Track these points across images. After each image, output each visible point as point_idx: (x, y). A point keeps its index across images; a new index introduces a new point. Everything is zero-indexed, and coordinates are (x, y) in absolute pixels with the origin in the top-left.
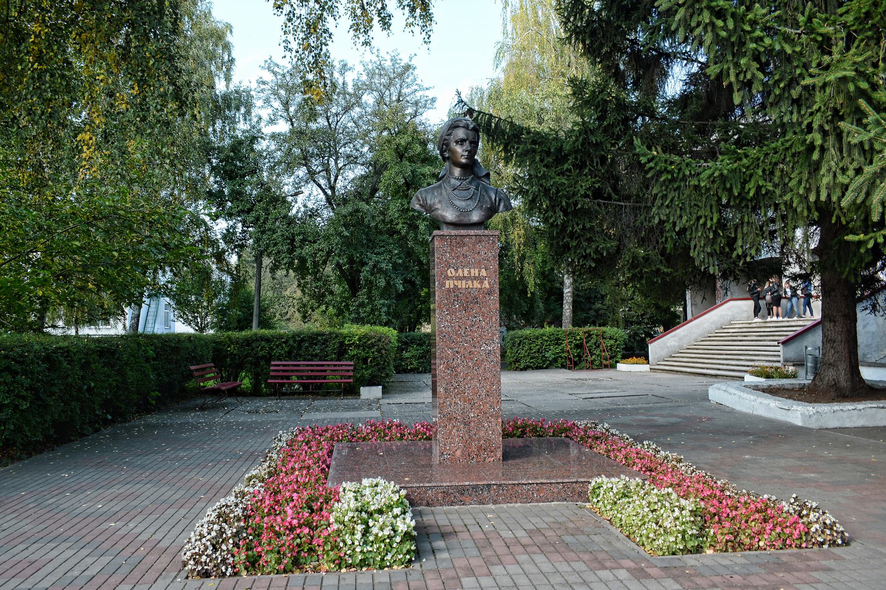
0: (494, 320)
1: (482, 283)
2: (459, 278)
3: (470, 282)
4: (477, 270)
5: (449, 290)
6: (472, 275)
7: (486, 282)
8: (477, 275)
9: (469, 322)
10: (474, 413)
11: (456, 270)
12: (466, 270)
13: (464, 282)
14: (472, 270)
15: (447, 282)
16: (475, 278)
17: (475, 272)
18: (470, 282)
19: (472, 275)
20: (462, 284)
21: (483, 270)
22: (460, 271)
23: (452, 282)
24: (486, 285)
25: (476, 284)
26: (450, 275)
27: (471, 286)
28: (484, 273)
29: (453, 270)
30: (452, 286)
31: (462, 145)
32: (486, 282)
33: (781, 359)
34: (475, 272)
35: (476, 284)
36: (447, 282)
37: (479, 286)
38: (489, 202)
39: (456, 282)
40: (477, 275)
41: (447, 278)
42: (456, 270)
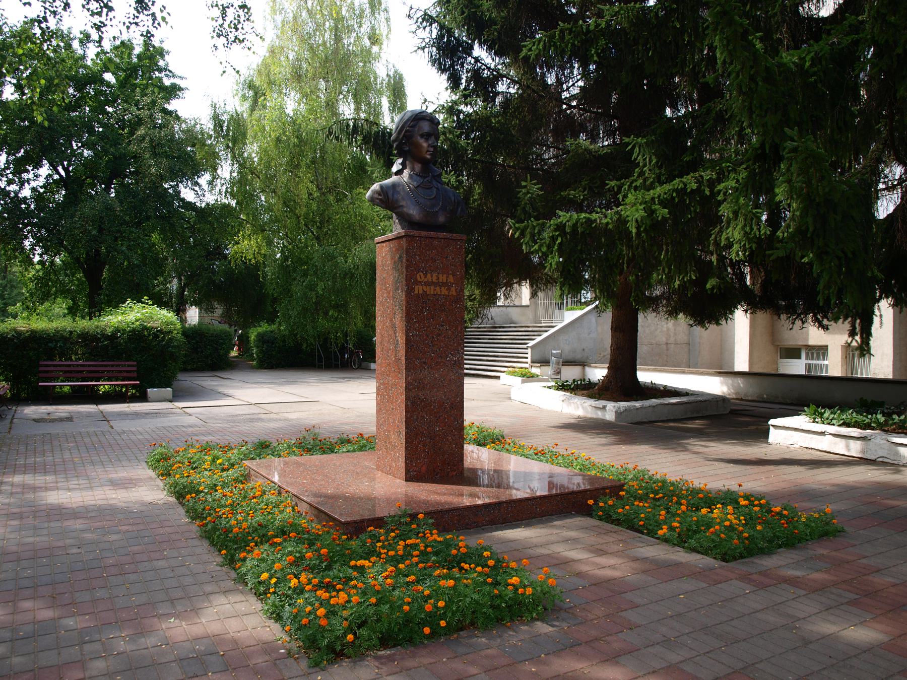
1: (449, 289)
2: (428, 284)
3: (438, 288)
5: (418, 295)
7: (453, 289)
10: (439, 426)
11: (425, 275)
12: (434, 275)
13: (432, 288)
15: (416, 287)
16: (444, 284)
17: (443, 278)
18: (438, 288)
20: (430, 290)
21: (451, 276)
22: (429, 275)
23: (421, 288)
25: (444, 291)
26: (419, 279)
28: (451, 279)
30: (421, 292)
31: (427, 140)
33: (529, 360)
34: (443, 278)
35: (444, 291)
36: (416, 287)
41: (417, 282)
42: (425, 275)
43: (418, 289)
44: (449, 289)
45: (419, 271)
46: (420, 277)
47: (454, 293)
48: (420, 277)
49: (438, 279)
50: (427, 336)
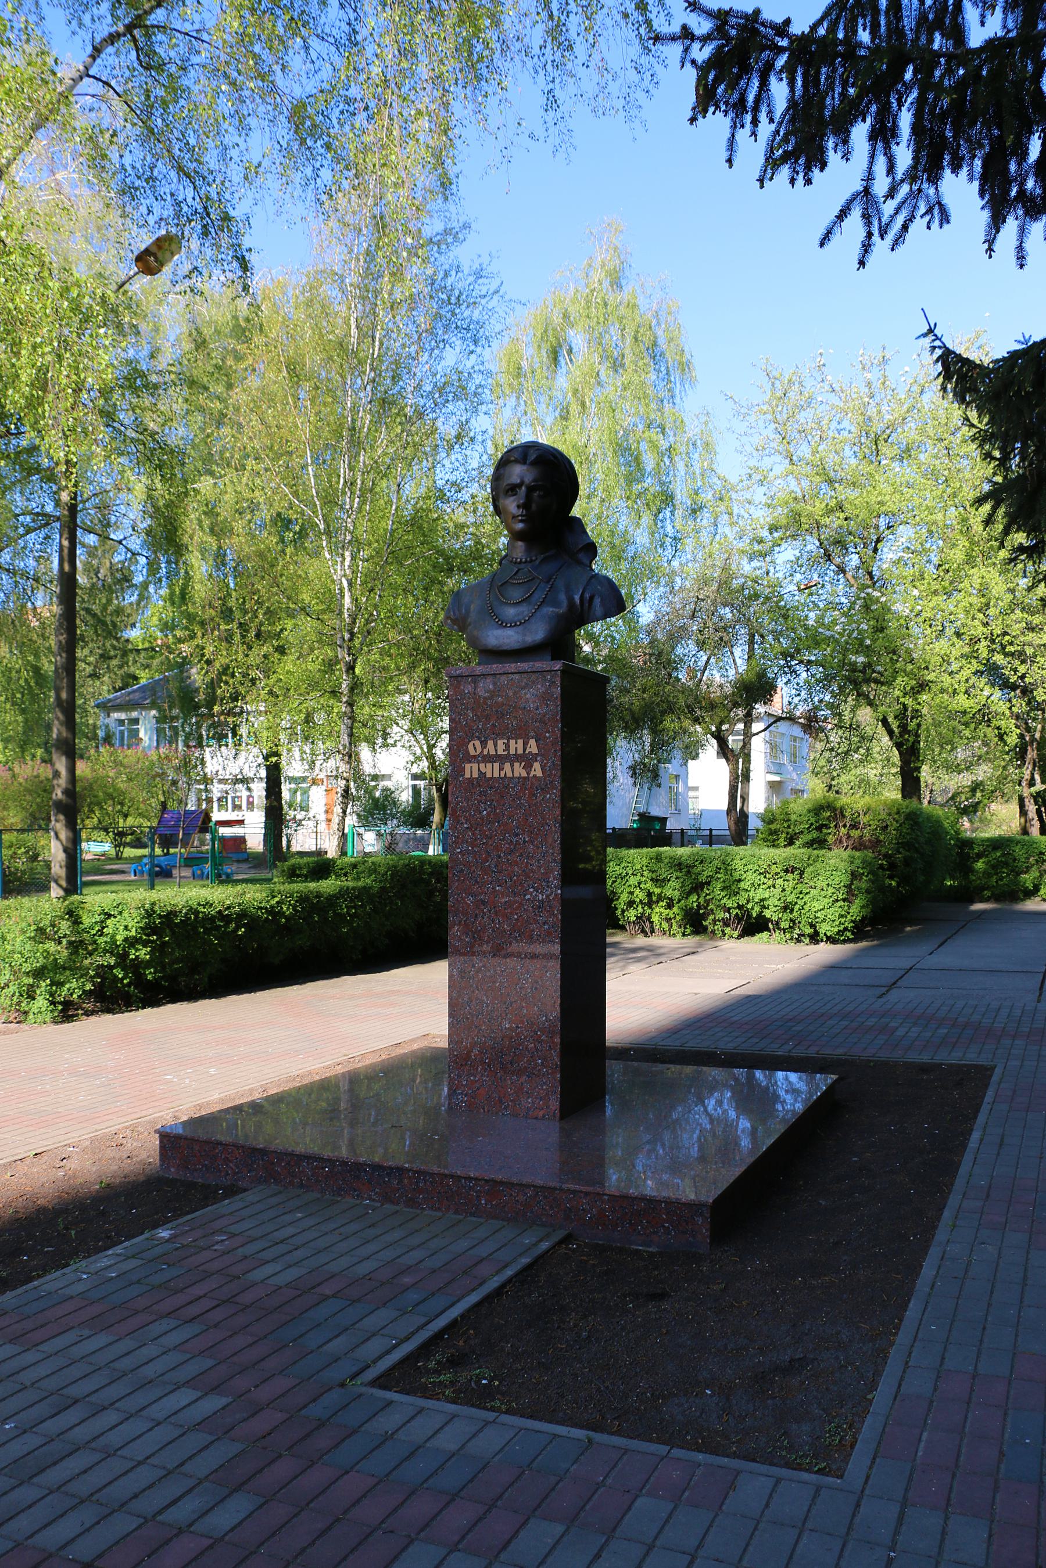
0: (550, 840)
1: (528, 767)
2: (489, 759)
3: (507, 766)
4: (520, 742)
6: (512, 751)
7: (537, 765)
8: (520, 751)
9: (505, 846)
11: (484, 744)
13: (497, 765)
14: (512, 742)
15: (468, 766)
16: (518, 758)
17: (516, 746)
19: (512, 751)
20: (493, 770)
21: (532, 742)
22: (490, 743)
23: (475, 766)
24: (537, 770)
26: (472, 752)
28: (533, 747)
29: (477, 743)
30: (475, 775)
32: (537, 765)
35: (519, 770)
36: (468, 766)
37: (524, 774)
38: (565, 604)
39: (482, 765)
40: (520, 751)
41: (470, 759)
42: (484, 744)
43: (471, 770)
44: (528, 767)
46: (474, 747)
47: (539, 774)
48: (474, 747)
49: (507, 746)
50: (488, 854)
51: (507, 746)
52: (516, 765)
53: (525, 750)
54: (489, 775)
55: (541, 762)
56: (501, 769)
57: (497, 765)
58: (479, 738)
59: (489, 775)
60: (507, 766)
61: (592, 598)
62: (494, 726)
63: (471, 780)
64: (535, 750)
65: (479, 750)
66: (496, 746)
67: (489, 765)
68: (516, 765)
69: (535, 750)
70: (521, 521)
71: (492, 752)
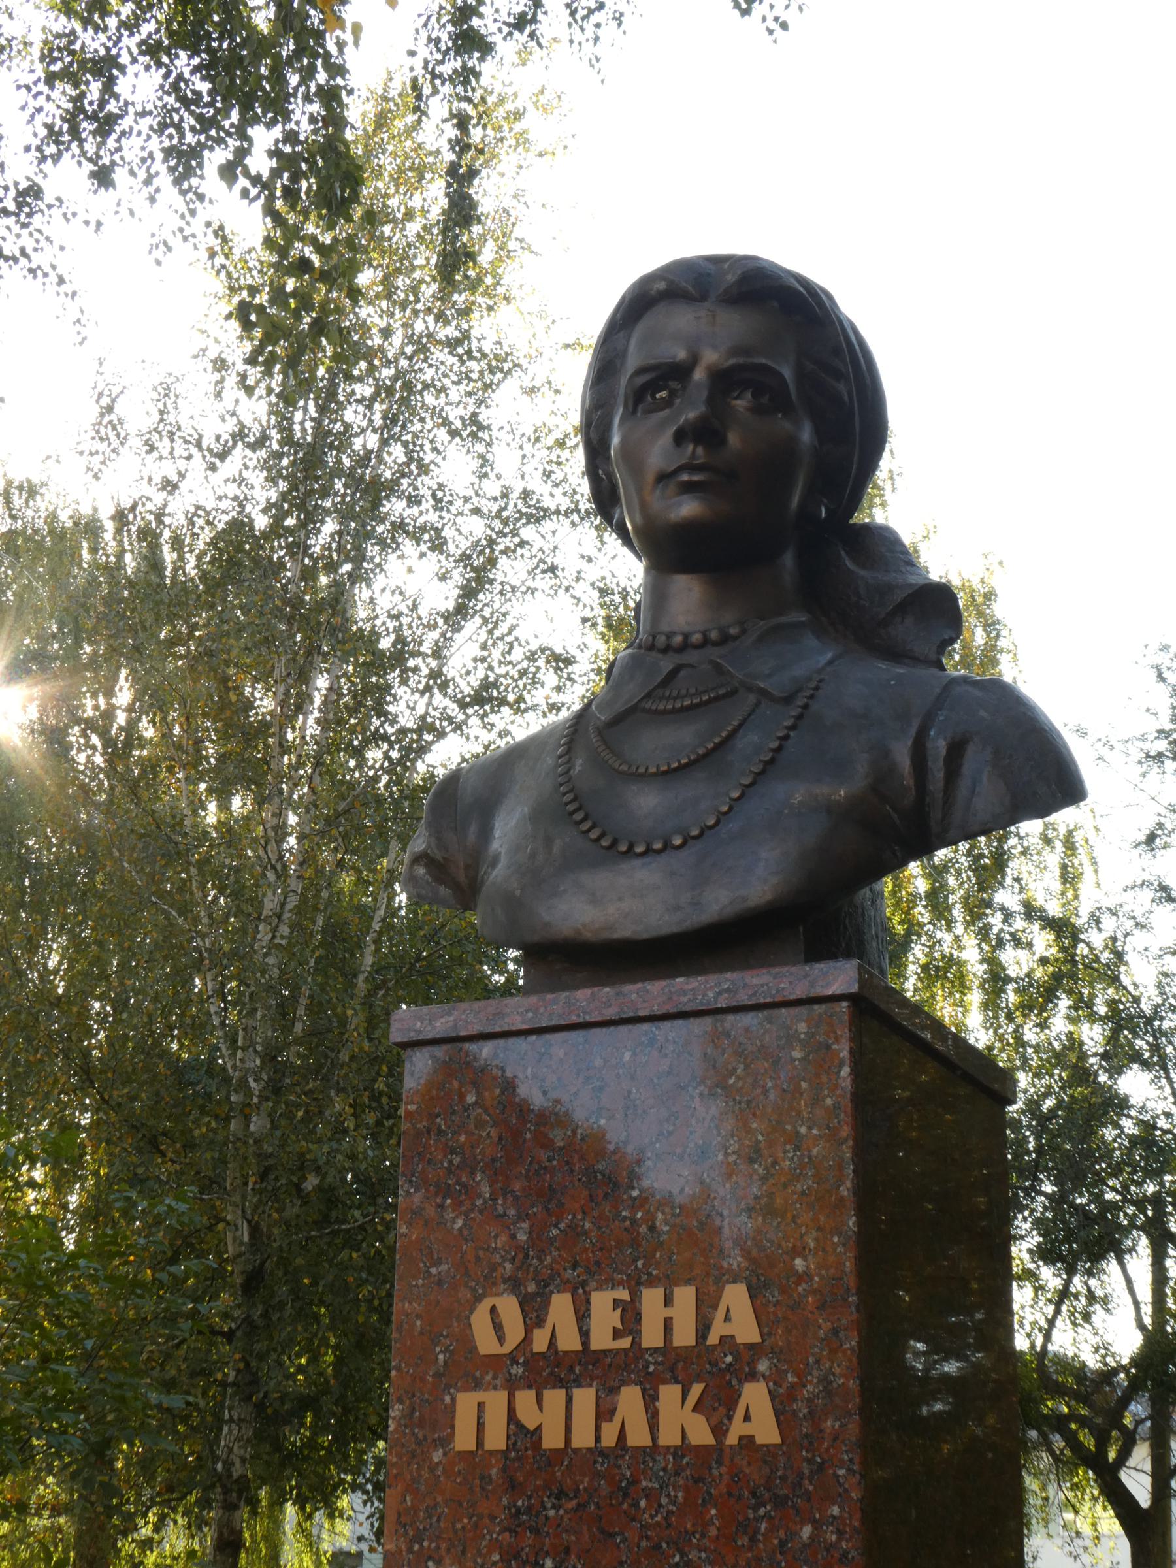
1: (720, 1403)
3: (630, 1399)
4: (685, 1295)
6: (652, 1337)
7: (755, 1396)
8: (684, 1336)
11: (534, 1312)
12: (602, 1303)
13: (585, 1398)
14: (652, 1298)
15: (466, 1403)
16: (674, 1365)
20: (566, 1419)
21: (736, 1297)
22: (561, 1306)
23: (496, 1401)
24: (757, 1416)
26: (486, 1343)
27: (639, 1437)
28: (739, 1318)
29: (509, 1307)
30: (496, 1439)
32: (755, 1396)
34: (668, 1316)
35: (681, 1419)
36: (466, 1403)
37: (701, 1434)
39: (525, 1399)
40: (684, 1336)
41: (471, 1369)
42: (534, 1312)
44: (720, 1403)
45: (488, 1284)
47: (766, 1431)
49: (631, 1316)
51: (631, 1316)
52: (669, 1394)
53: (703, 1329)
54: (552, 1440)
55: (775, 1379)
56: (604, 1413)
57: (585, 1398)
58: (514, 1284)
59: (552, 1440)
60: (630, 1399)
61: (956, 750)
62: (574, 1232)
63: (476, 1458)
64: (746, 1330)
65: (515, 1332)
66: (582, 1315)
67: (554, 1397)
68: (669, 1394)
69: (746, 1330)
70: (689, 488)
71: (569, 1341)
